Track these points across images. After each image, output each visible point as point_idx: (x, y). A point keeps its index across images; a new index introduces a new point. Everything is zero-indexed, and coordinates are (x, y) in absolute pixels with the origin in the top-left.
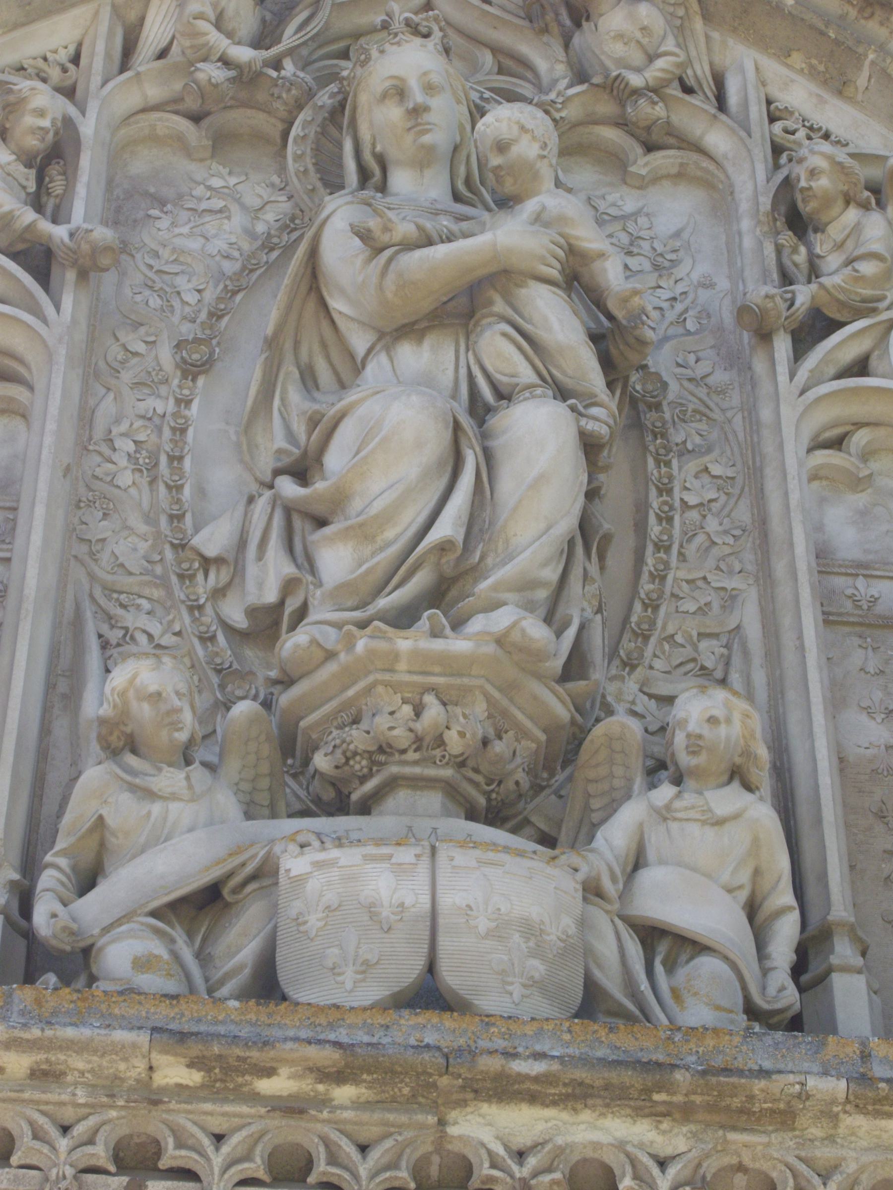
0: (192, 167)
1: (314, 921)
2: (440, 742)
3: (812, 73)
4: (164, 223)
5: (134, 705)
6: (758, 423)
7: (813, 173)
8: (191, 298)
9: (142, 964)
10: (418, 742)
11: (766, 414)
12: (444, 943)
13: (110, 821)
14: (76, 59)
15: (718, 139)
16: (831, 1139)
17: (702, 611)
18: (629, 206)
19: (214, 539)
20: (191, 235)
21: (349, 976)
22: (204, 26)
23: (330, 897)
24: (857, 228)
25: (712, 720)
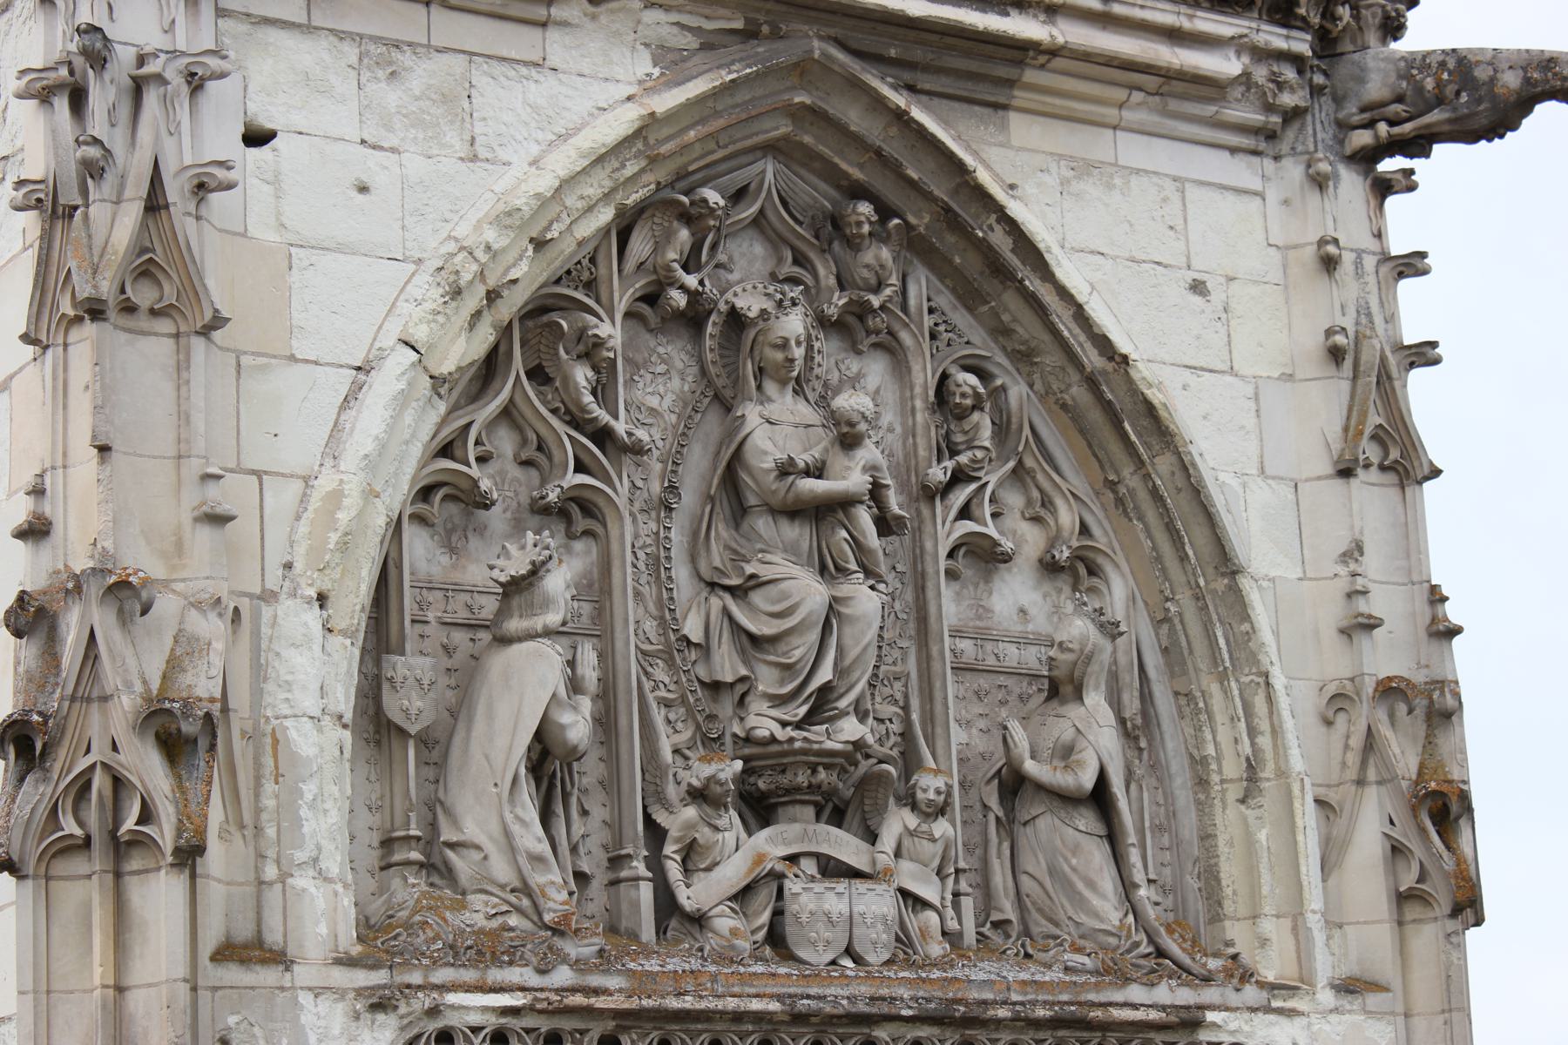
0: (648, 336)
1: (804, 918)
2: (819, 787)
3: (954, 291)
4: (641, 385)
5: (712, 786)
6: (922, 548)
7: (963, 395)
8: (660, 444)
9: (734, 932)
10: (810, 786)
11: (929, 545)
12: (855, 930)
13: (701, 841)
14: (593, 260)
15: (905, 337)
16: (997, 1029)
17: (894, 663)
18: (855, 368)
19: (693, 628)
20: (652, 394)
21: (820, 948)
22: (676, 265)
23: (812, 906)
24: (977, 427)
25: (938, 792)
